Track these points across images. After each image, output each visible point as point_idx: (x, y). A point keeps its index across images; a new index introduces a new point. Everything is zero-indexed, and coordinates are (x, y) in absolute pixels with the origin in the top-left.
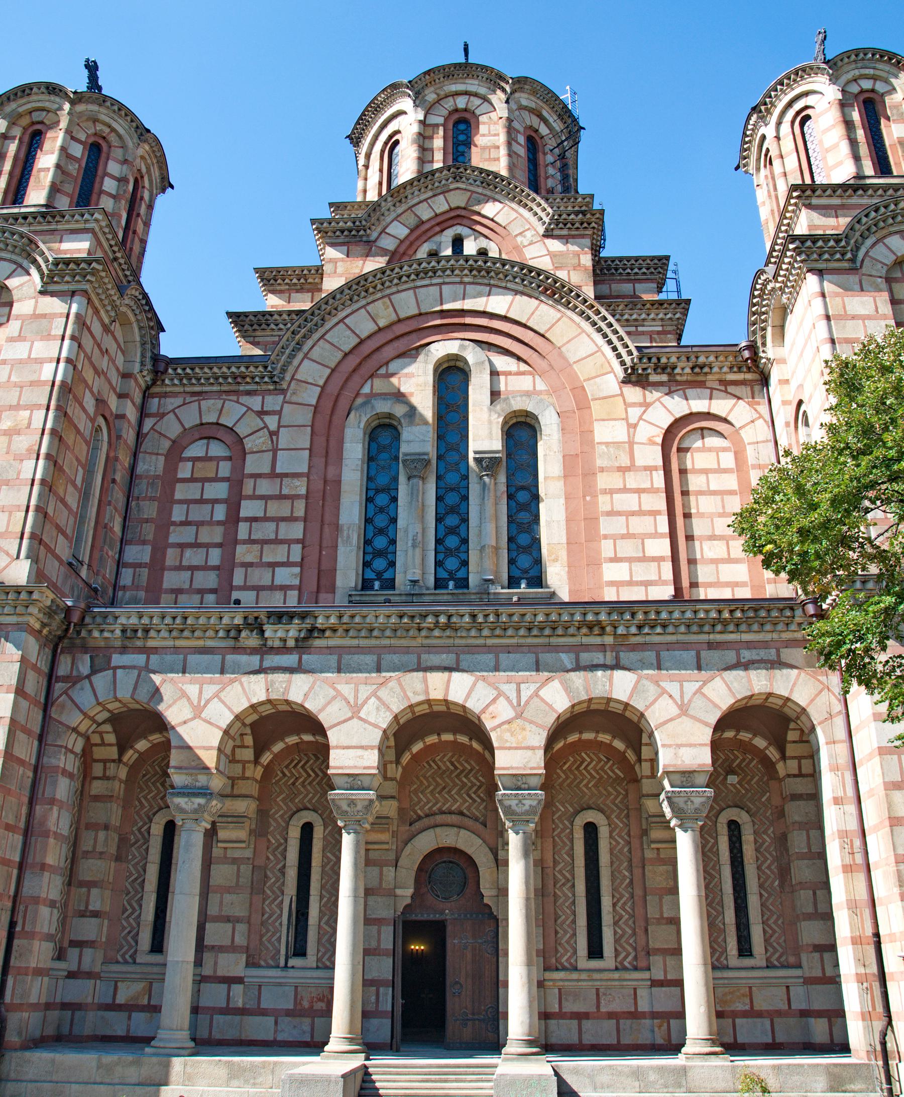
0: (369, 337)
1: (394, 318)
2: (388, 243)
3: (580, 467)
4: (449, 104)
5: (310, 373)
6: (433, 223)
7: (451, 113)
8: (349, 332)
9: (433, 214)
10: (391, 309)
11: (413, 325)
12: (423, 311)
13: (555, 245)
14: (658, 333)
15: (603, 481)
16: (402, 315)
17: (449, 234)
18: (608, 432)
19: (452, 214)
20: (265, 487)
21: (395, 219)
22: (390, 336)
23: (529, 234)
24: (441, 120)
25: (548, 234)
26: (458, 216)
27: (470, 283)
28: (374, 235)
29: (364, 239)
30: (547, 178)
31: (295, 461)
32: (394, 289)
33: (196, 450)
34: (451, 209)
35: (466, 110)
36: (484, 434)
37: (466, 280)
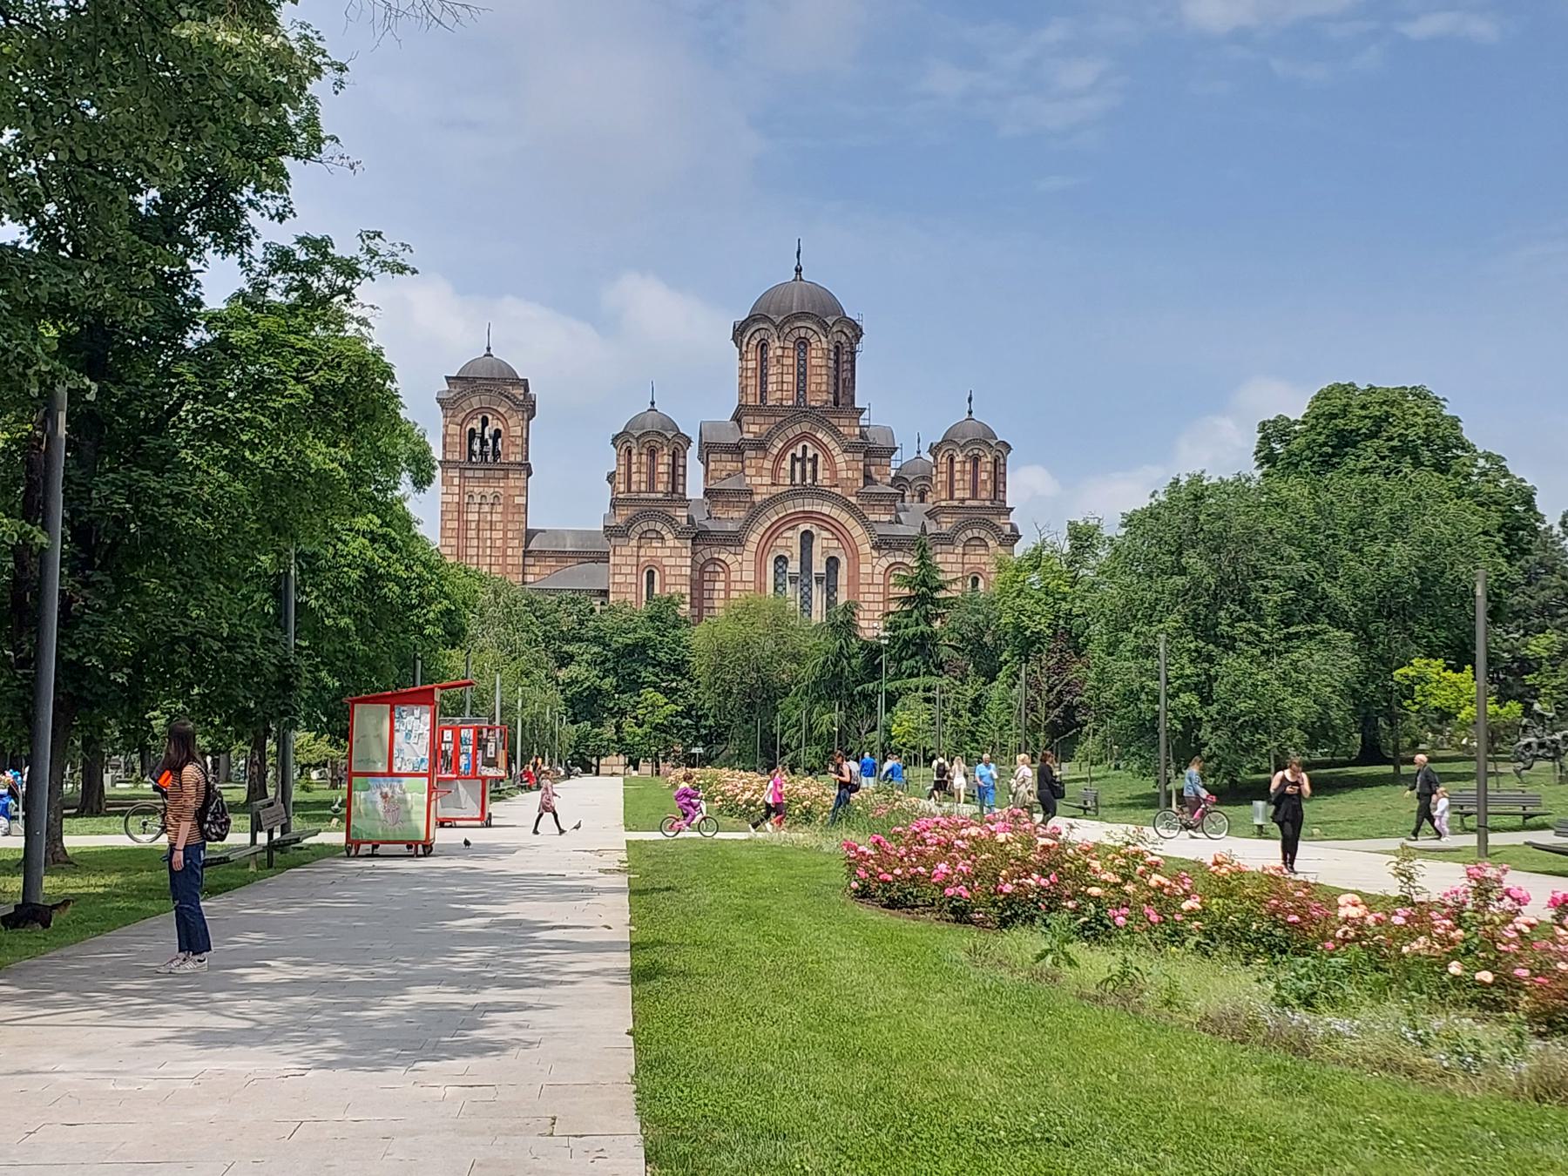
2: (775, 451)
3: (853, 580)
5: (754, 538)
13: (848, 456)
15: (863, 589)
17: (800, 447)
18: (865, 569)
20: (739, 586)
31: (749, 575)
33: (710, 568)
36: (819, 567)
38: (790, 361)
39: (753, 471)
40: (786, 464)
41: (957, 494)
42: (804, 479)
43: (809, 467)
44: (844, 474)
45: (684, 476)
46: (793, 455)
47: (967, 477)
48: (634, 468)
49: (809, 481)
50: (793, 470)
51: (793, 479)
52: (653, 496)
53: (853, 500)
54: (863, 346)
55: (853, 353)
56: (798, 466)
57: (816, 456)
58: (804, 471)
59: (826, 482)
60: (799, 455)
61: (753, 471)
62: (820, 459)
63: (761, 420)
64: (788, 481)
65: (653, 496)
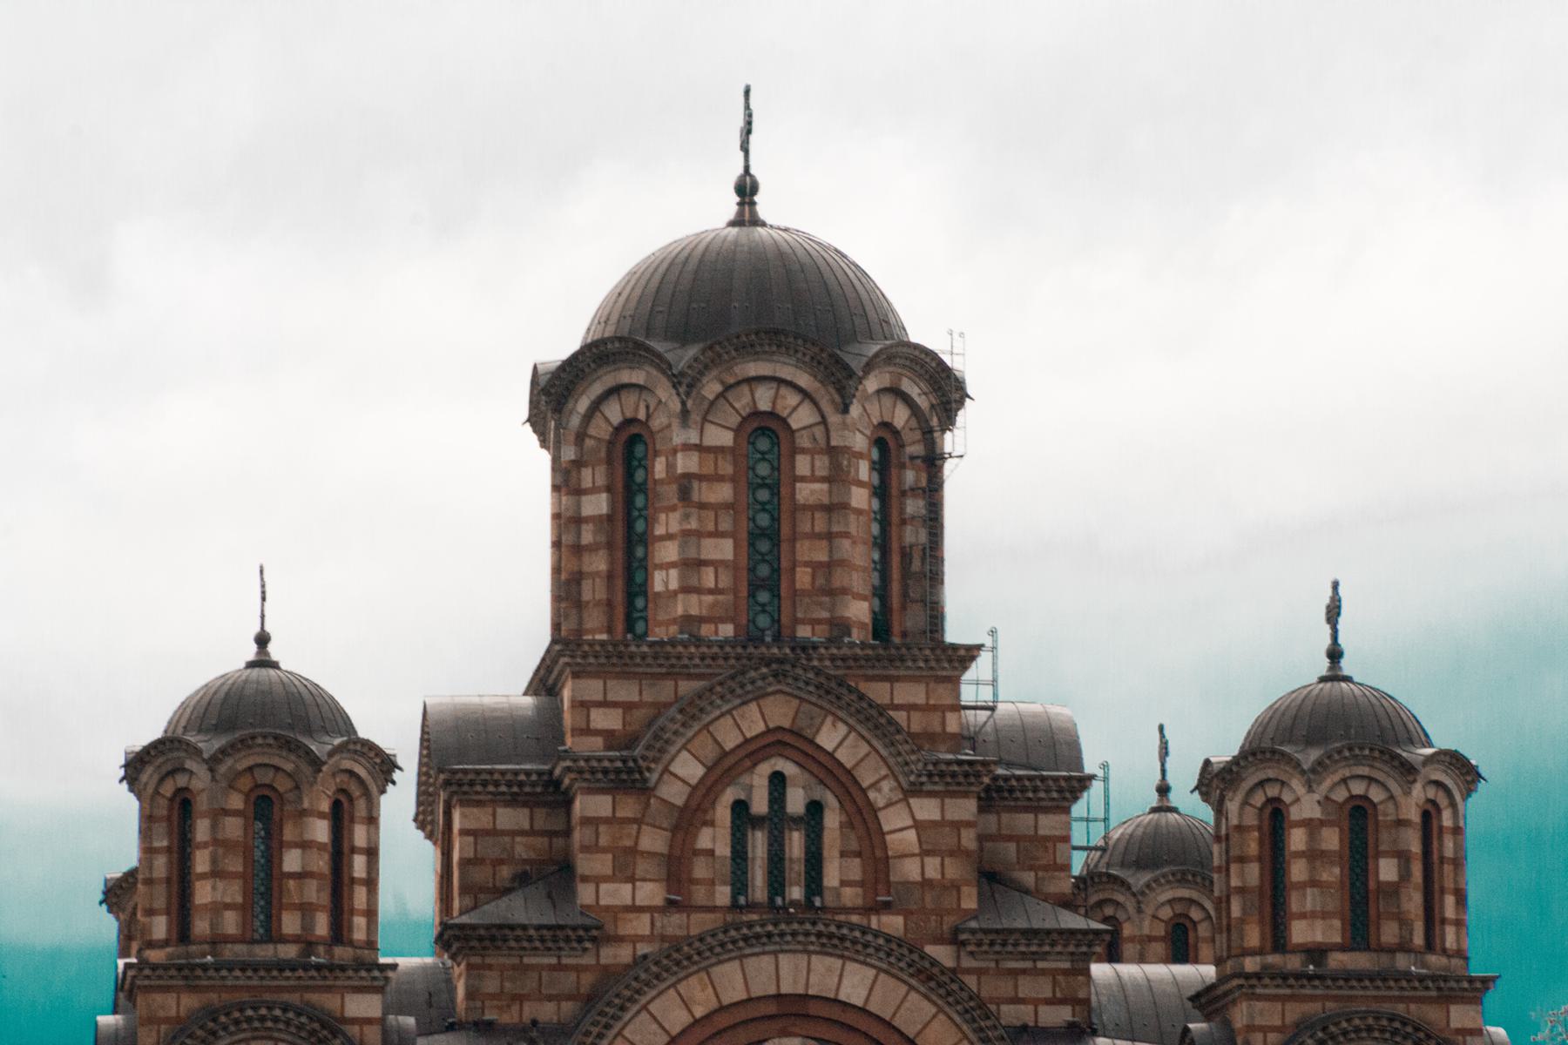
0: (683, 1032)
1: (714, 1004)
2: (674, 793)
4: (742, 401)
6: (742, 753)
7: (745, 419)
8: (655, 1026)
9: (740, 739)
10: (710, 989)
11: (743, 1014)
12: (753, 995)
13: (927, 809)
14: (1065, 972)
16: (726, 1001)
17: (765, 769)
19: (771, 738)
21: (684, 747)
22: (709, 1031)
23: (886, 786)
24: (725, 438)
25: (913, 791)
26: (779, 742)
27: (817, 953)
28: (654, 777)
29: (638, 785)
30: (903, 522)
32: (714, 960)
34: (769, 731)
35: (772, 414)
37: (811, 948)
38: (724, 492)
39: (599, 864)
40: (715, 839)
41: (1300, 932)
42: (777, 882)
43: (796, 843)
44: (910, 870)
45: (371, 883)
46: (740, 807)
47: (1332, 874)
48: (201, 862)
49: (796, 893)
50: (740, 854)
51: (740, 883)
52: (264, 952)
53: (943, 954)
54: (965, 440)
55: (933, 461)
56: (758, 843)
57: (815, 809)
58: (776, 860)
59: (851, 896)
60: (760, 806)
61: (599, 864)
62: (832, 820)
63: (625, 691)
64: (723, 895)
65: (264, 952)
